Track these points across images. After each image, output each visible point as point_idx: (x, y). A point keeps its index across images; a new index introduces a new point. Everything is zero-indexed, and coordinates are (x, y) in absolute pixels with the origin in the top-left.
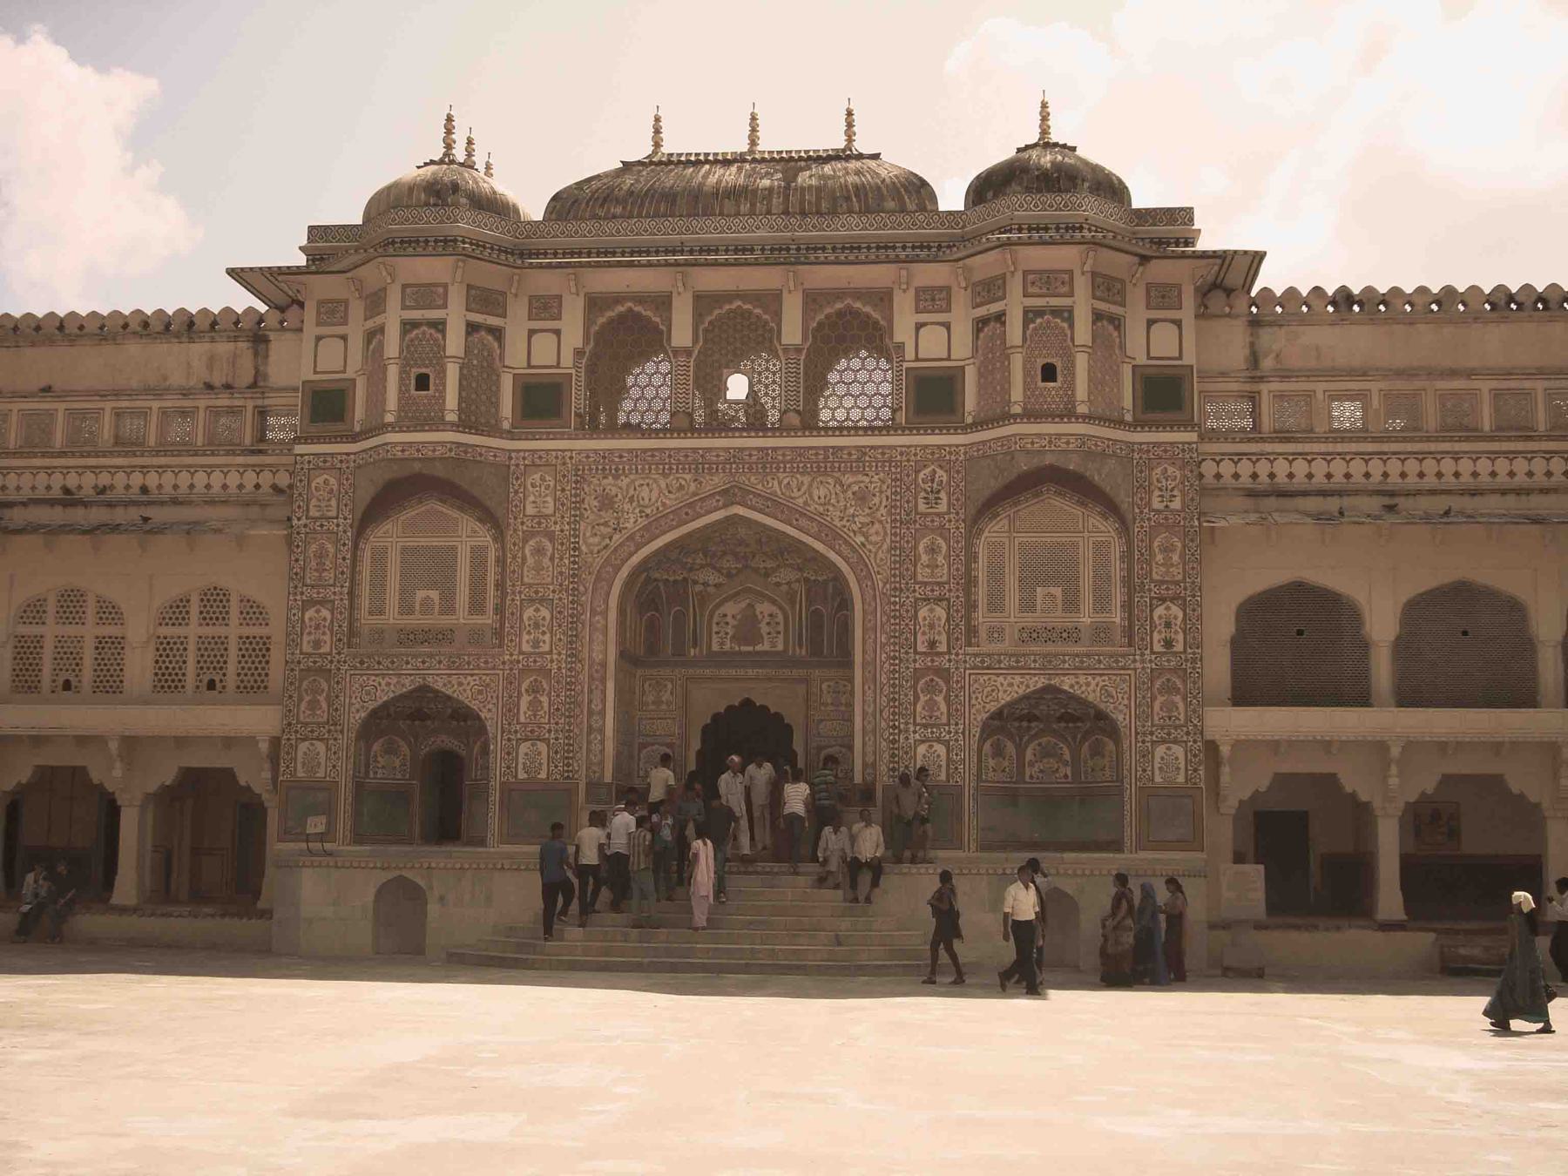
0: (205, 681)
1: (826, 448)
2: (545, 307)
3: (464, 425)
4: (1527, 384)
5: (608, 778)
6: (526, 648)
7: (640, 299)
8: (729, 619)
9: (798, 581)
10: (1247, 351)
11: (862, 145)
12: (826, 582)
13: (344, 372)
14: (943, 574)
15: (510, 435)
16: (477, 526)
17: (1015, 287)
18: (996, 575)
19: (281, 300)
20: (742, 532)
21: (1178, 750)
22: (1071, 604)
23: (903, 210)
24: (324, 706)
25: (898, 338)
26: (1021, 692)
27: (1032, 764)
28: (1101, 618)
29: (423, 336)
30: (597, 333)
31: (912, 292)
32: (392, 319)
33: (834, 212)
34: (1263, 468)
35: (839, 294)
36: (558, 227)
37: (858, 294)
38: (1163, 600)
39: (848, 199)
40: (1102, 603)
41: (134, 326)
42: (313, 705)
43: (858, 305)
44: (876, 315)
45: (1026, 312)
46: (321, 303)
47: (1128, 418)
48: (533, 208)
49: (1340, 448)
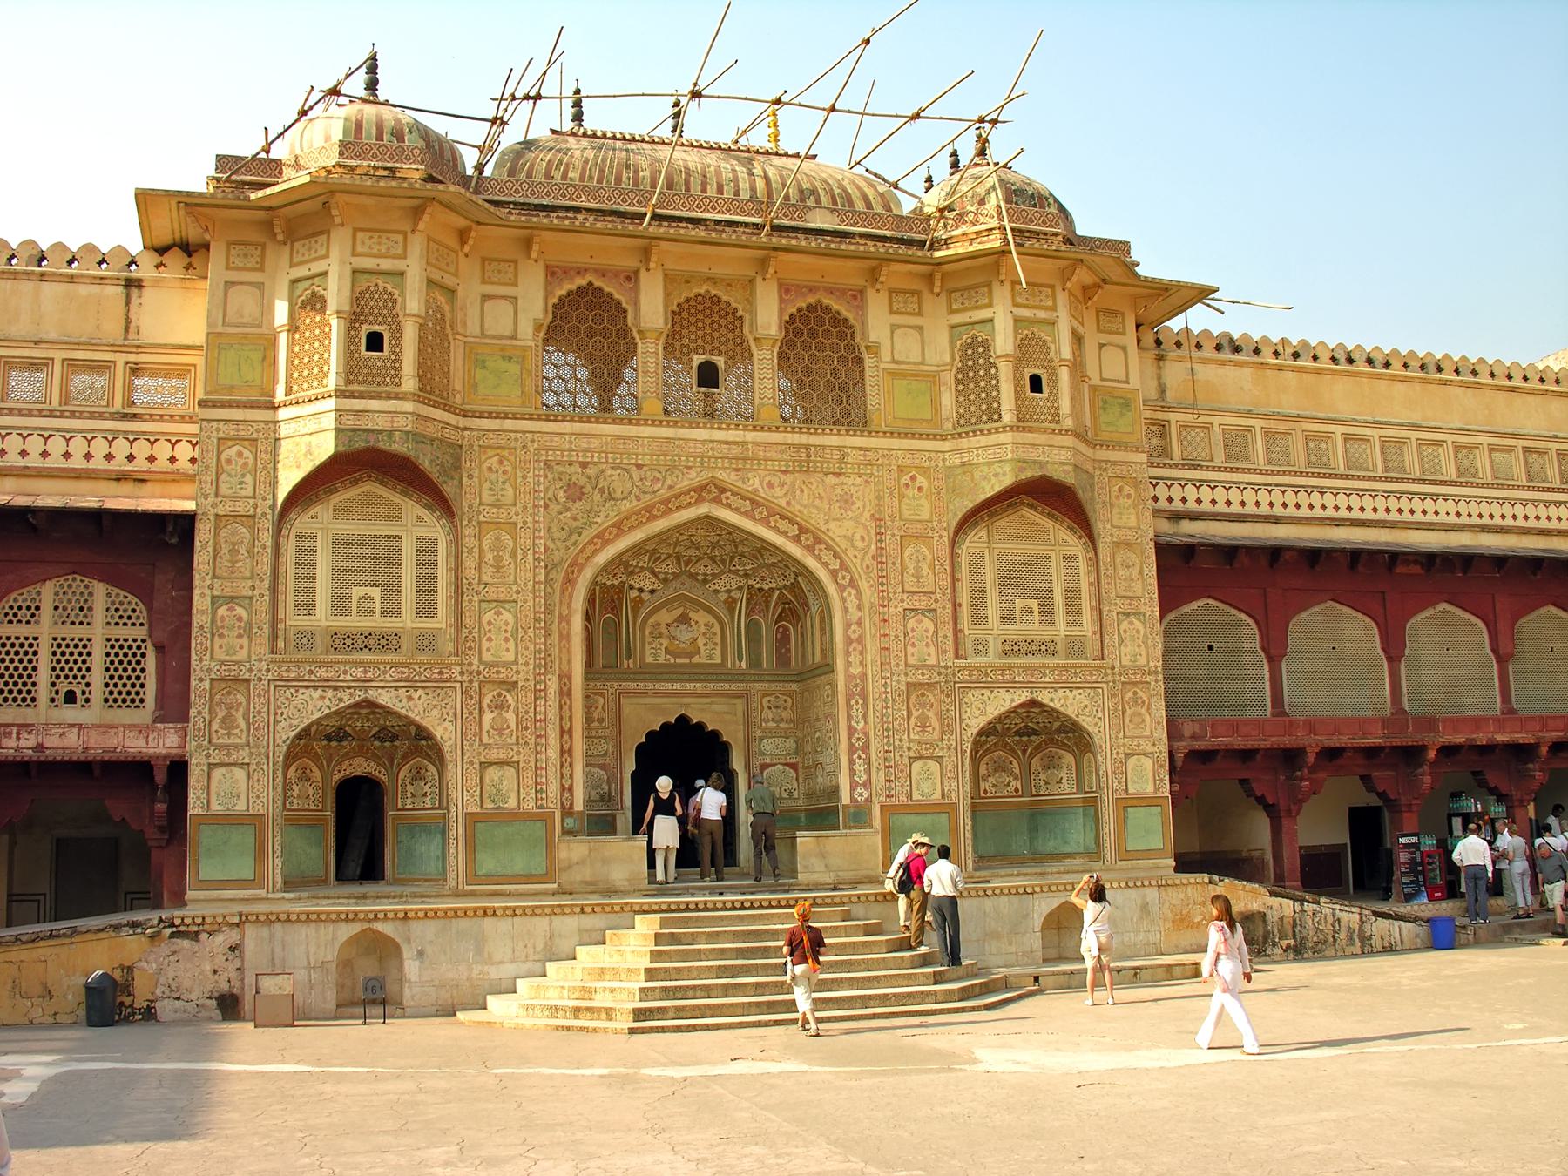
0: (63, 687)
1: (807, 447)
4: (1367, 431)
5: (579, 806)
6: (487, 657)
8: (663, 629)
9: (740, 588)
10: (1155, 383)
12: (772, 590)
13: (260, 326)
14: (928, 582)
16: (424, 513)
18: (978, 587)
19: (164, 236)
20: (700, 535)
21: (1148, 763)
22: (1048, 618)
24: (243, 725)
25: (873, 338)
26: (1007, 706)
27: (986, 780)
28: (1076, 632)
30: (555, 306)
31: (884, 296)
34: (1176, 492)
38: (1128, 615)
39: (814, 192)
40: (1074, 617)
42: (229, 723)
43: (826, 301)
44: (845, 314)
45: (1017, 320)
46: (230, 244)
49: (1235, 477)
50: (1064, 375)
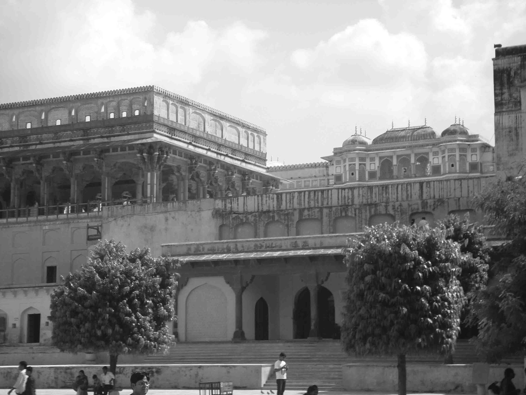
2: (372, 159)
3: (359, 181)
7: (388, 157)
11: (428, 125)
15: (368, 181)
17: (446, 151)
23: (431, 138)
29: (352, 167)
32: (347, 163)
33: (419, 139)
35: (420, 154)
36: (373, 145)
37: (423, 153)
41: (306, 166)
47: (468, 171)
48: (370, 142)
50: (458, 164)
